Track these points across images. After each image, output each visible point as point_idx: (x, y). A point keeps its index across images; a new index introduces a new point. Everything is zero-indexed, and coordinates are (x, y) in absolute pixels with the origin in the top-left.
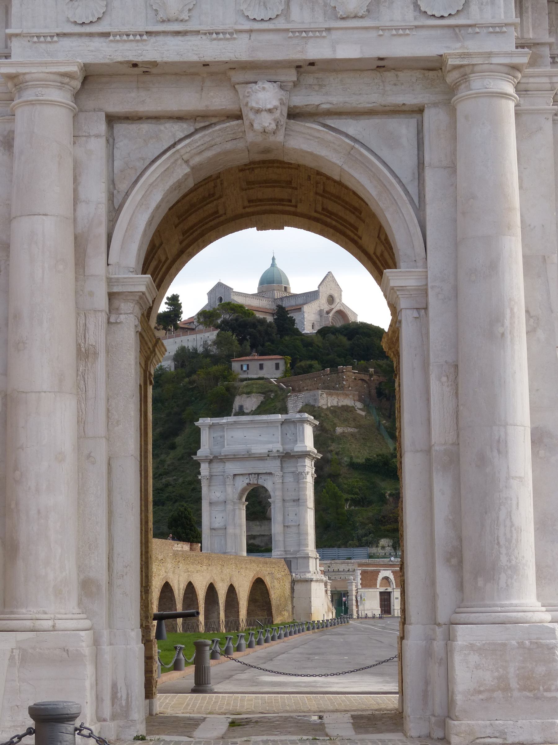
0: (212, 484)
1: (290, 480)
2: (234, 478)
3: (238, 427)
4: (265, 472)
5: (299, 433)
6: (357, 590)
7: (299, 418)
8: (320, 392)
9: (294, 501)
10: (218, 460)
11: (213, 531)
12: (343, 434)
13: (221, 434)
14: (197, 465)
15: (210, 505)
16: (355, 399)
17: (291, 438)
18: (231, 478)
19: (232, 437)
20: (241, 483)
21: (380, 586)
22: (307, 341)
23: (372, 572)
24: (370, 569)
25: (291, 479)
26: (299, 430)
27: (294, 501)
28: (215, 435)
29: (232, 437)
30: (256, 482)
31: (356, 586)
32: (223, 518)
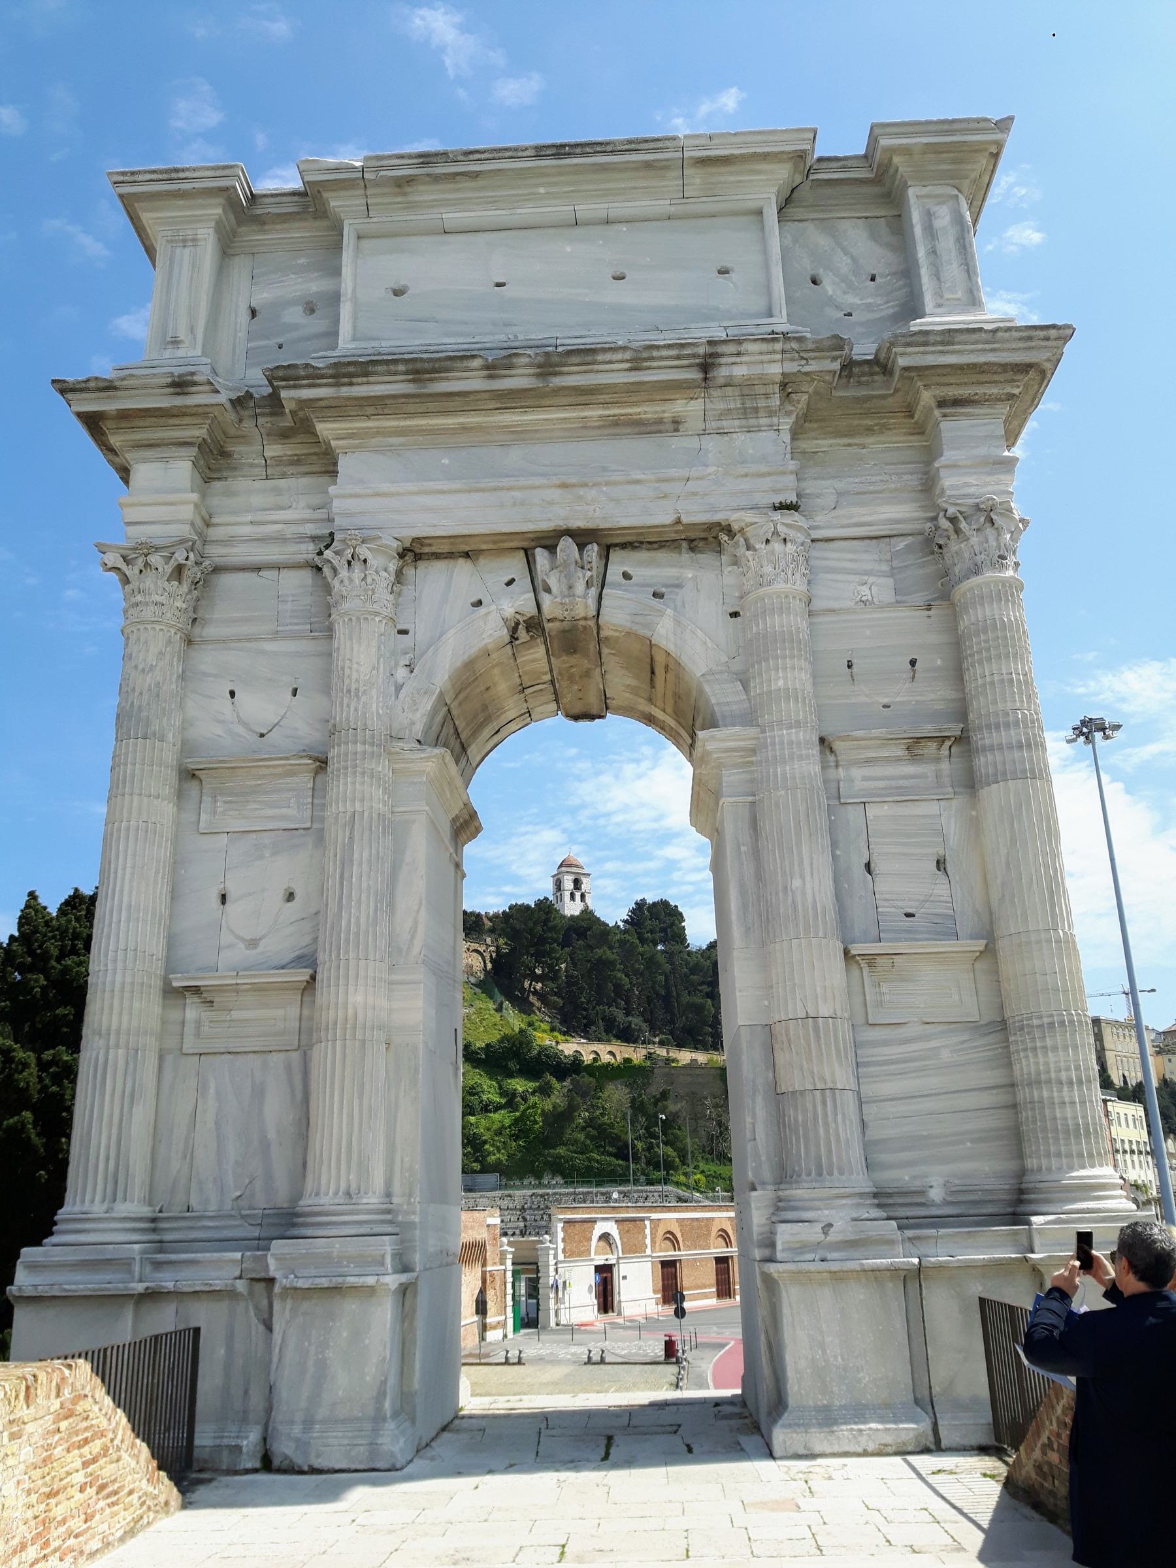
0: (210, 631)
3: (452, 217)
4: (668, 519)
5: (934, 252)
6: (556, 1264)
10: (274, 450)
11: (193, 1011)
13: (316, 285)
15: (180, 795)
17: (852, 299)
18: (383, 565)
19: (398, 293)
21: (596, 1254)
25: (881, 589)
26: (931, 232)
28: (262, 297)
29: (398, 293)
31: (555, 1256)
32: (290, 897)
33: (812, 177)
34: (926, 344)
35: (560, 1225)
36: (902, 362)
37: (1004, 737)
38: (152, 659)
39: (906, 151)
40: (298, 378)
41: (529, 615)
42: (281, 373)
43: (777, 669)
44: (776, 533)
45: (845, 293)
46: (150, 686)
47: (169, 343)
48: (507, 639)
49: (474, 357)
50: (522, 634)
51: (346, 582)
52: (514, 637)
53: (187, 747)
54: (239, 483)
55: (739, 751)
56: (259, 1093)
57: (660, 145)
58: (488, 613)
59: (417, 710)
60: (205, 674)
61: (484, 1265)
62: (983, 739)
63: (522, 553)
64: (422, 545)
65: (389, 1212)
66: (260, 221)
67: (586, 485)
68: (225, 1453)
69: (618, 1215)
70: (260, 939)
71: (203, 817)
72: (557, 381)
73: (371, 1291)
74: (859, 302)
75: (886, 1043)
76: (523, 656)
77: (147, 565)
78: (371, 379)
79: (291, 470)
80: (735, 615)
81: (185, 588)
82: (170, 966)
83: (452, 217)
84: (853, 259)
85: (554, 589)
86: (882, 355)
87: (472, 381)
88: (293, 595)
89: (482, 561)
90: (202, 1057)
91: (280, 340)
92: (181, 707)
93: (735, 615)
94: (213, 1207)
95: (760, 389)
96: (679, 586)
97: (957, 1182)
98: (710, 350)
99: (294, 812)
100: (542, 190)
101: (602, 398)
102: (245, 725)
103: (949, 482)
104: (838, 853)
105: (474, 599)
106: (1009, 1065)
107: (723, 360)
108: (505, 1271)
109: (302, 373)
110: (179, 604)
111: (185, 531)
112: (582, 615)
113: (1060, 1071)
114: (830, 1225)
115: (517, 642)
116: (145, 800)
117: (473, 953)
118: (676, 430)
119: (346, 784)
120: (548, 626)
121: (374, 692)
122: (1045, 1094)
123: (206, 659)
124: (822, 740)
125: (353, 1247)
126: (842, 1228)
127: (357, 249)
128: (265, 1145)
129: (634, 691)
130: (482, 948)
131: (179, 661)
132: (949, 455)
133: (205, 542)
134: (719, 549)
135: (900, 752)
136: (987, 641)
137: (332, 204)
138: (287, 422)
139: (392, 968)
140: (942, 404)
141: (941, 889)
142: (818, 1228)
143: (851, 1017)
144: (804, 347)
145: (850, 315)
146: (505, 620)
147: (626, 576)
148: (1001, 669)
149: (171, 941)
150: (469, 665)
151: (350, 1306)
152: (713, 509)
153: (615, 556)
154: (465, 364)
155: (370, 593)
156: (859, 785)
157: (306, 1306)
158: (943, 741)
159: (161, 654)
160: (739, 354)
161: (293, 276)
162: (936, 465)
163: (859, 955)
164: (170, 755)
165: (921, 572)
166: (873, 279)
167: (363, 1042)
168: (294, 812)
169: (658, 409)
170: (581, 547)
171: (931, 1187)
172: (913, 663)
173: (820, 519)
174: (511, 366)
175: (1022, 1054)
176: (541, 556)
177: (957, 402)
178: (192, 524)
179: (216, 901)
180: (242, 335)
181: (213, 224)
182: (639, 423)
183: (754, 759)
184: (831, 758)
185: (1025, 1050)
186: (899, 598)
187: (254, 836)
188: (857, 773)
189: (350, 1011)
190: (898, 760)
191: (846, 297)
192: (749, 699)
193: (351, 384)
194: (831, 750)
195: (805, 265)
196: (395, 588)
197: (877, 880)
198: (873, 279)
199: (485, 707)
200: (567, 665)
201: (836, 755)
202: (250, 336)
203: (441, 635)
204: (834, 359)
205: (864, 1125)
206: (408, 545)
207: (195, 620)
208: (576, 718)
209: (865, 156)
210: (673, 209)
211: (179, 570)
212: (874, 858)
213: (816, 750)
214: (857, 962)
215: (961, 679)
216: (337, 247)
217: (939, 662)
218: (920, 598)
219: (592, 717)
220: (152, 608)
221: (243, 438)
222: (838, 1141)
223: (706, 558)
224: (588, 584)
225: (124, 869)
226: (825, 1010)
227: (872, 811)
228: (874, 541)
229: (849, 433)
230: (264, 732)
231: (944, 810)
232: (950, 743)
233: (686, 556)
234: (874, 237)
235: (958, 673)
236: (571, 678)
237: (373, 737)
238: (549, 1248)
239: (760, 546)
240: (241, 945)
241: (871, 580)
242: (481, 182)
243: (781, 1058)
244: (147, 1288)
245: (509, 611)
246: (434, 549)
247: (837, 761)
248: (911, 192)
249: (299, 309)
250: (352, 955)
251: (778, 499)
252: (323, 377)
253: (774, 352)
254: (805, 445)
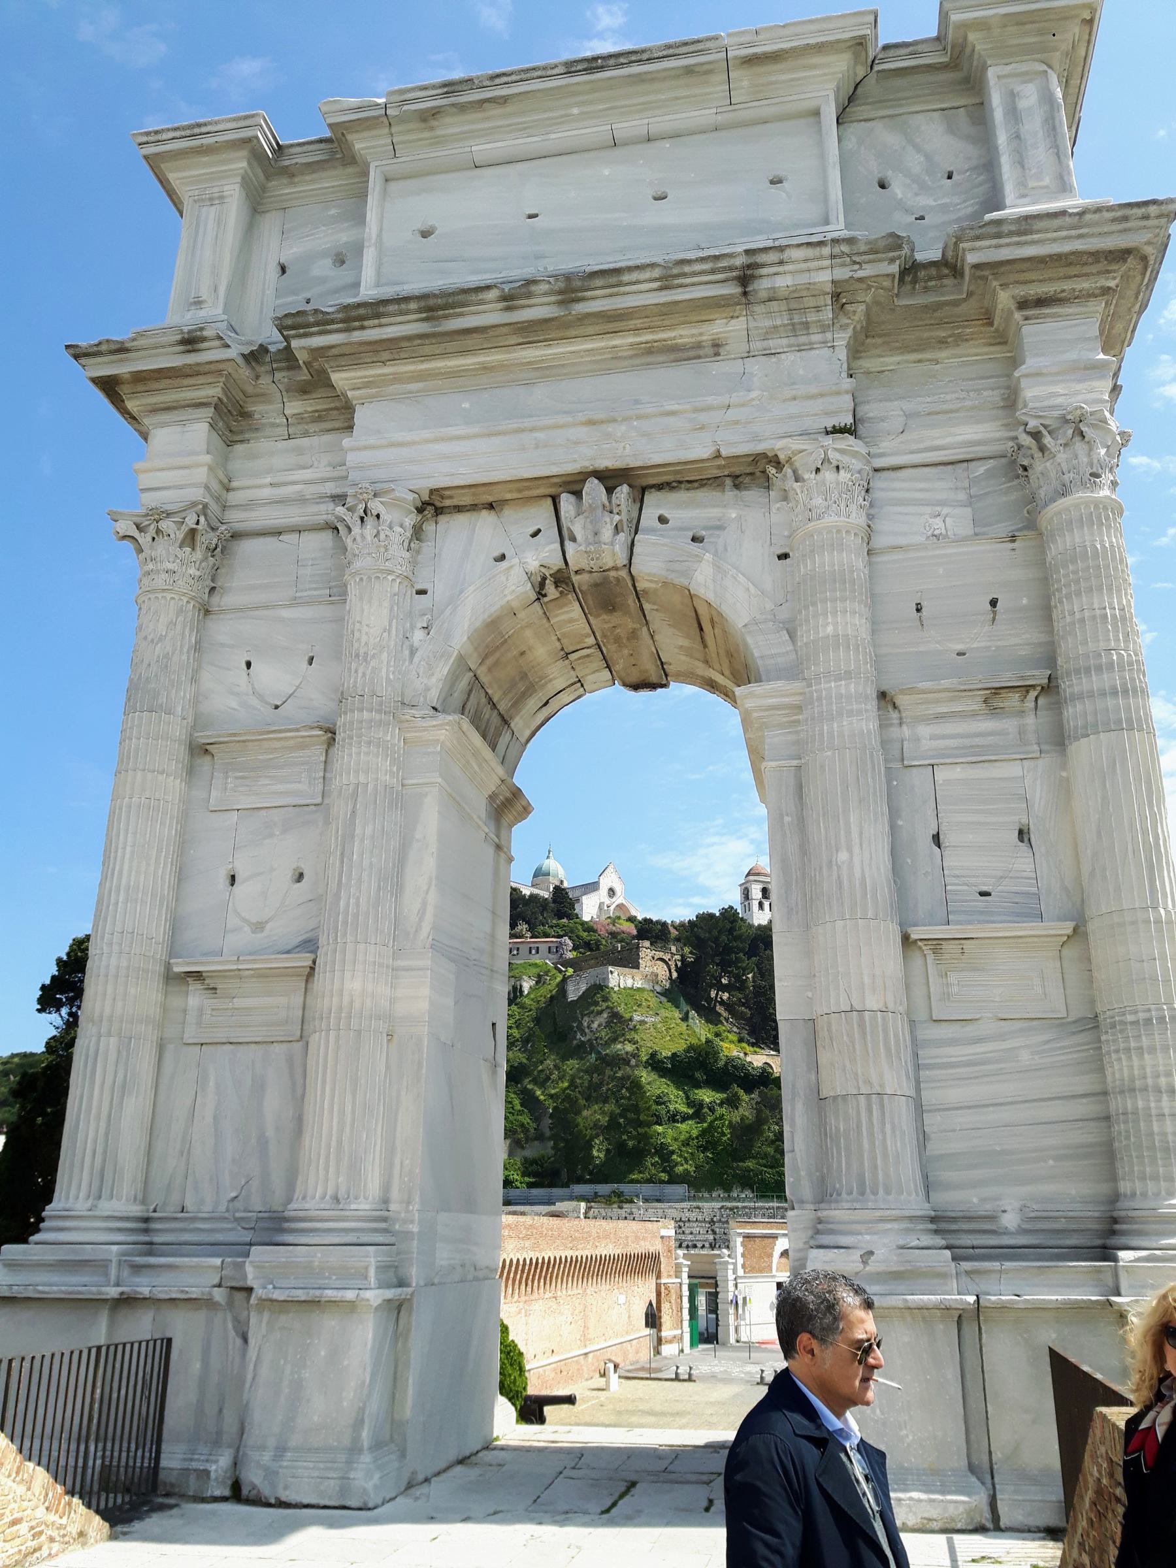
1: (938, 525)
2: (418, 532)
3: (482, 149)
6: (735, 1279)
8: (610, 968)
10: (294, 407)
11: (195, 998)
12: (642, 1022)
13: (344, 236)
15: (191, 772)
17: (925, 201)
19: (425, 234)
22: (589, 928)
25: (957, 521)
26: (1013, 114)
29: (425, 234)
33: (876, 68)
34: (999, 236)
35: (739, 1240)
36: (971, 258)
37: (1096, 682)
38: (161, 629)
39: (982, 25)
40: (308, 326)
41: (555, 568)
42: (289, 322)
43: (825, 614)
44: (826, 460)
45: (916, 195)
46: (159, 657)
47: (191, 304)
48: (533, 596)
49: (488, 288)
50: (551, 591)
51: (359, 539)
52: (541, 594)
53: (199, 722)
54: (261, 445)
55: (783, 709)
56: (259, 1087)
57: (700, 46)
58: (511, 567)
59: (433, 674)
60: (222, 645)
61: (659, 1277)
62: (1071, 686)
63: (549, 501)
64: (443, 498)
65: (385, 1219)
66: (289, 173)
67: (614, 420)
68: (192, 1478)
70: (267, 922)
71: (214, 794)
72: (581, 308)
73: (351, 1307)
74: (934, 203)
75: (954, 1042)
76: (557, 616)
77: (158, 531)
78: (383, 321)
79: (313, 428)
80: (784, 556)
81: (199, 555)
82: (173, 951)
83: (482, 149)
84: (928, 157)
85: (579, 537)
86: (950, 254)
87: (489, 315)
88: (312, 559)
89: (507, 512)
90: (204, 1046)
91: (308, 295)
92: (194, 680)
93: (784, 556)
94: (208, 1207)
95: (810, 302)
96: (721, 528)
97: (1035, 1207)
98: (750, 260)
99: (305, 788)
100: (575, 111)
101: (632, 323)
102: (261, 698)
103: (1031, 392)
104: (900, 823)
105: (497, 554)
106: (1101, 1070)
107: (764, 271)
108: (681, 1284)
109: (311, 319)
110: (192, 571)
111: (198, 494)
112: (610, 564)
113: (1158, 1076)
114: (871, 1253)
115: (546, 599)
116: (149, 775)
117: (658, 962)
118: (717, 354)
119: (350, 755)
120: (576, 579)
121: (385, 656)
122: (1140, 1104)
123: (221, 630)
124: (883, 695)
125: (336, 1256)
126: (885, 1255)
127: (385, 192)
128: (263, 1143)
129: (689, 652)
130: (667, 957)
131: (191, 630)
132: (1031, 363)
133: (224, 508)
134: (767, 483)
135: (975, 704)
136: (1076, 572)
137: (357, 146)
138: (304, 375)
139: (395, 956)
140: (1023, 305)
141: (1022, 861)
142: (856, 1255)
143: (908, 1013)
144: (855, 249)
145: (922, 218)
146: (529, 576)
147: (663, 520)
148: (1093, 603)
149: (176, 925)
150: (493, 625)
151: (329, 1323)
152: (757, 439)
153: (650, 498)
154: (481, 296)
155: (382, 550)
156: (926, 745)
157: (284, 1320)
158: (1028, 692)
159: (172, 624)
160: (781, 263)
161: (323, 228)
162: (1016, 374)
163: (921, 940)
164: (177, 729)
165: (1004, 499)
166: (950, 177)
167: (359, 1032)
168: (305, 788)
169: (694, 331)
170: (610, 491)
171: (1004, 1211)
172: (994, 603)
173: (885, 445)
174: (529, 295)
175: (1114, 1056)
176: (567, 503)
177: (1041, 302)
178: (207, 487)
179: (223, 881)
180: (270, 292)
181: (239, 179)
182: (675, 349)
183: (801, 717)
184: (894, 715)
185: (1117, 1051)
186: (977, 530)
187: (263, 812)
188: (924, 731)
189: (346, 1000)
190: (974, 715)
191: (918, 198)
192: (795, 650)
193: (363, 328)
194: (895, 707)
195: (871, 168)
196: (412, 545)
197: (946, 853)
198: (950, 177)
199: (524, 676)
200: (610, 625)
201: (900, 711)
202: (279, 293)
203: (461, 592)
204: (892, 260)
205: (923, 1138)
206: (426, 498)
207: (213, 589)
208: (636, 687)
209: (938, 39)
210: (719, 117)
211: (192, 536)
212: (942, 828)
213: (872, 704)
214: (920, 948)
215: (1049, 618)
216: (363, 195)
217: (1025, 601)
218: (1003, 529)
219: (653, 686)
220: (164, 576)
221: (263, 397)
222: (885, 1155)
223: (753, 495)
224: (617, 529)
225: (124, 848)
226: (872, 1003)
227: (941, 775)
228: (950, 467)
229: (921, 346)
230: (279, 703)
231: (1028, 772)
232: (1036, 693)
233: (730, 494)
234: (951, 130)
235: (1046, 612)
236: (617, 640)
237: (381, 704)
238: (727, 1263)
239: (809, 476)
240: (247, 929)
241: (946, 510)
242: (509, 108)
243: (824, 1057)
244: (122, 1293)
245: (533, 564)
246: (455, 502)
247: (901, 718)
248: (991, 73)
249: (328, 262)
250: (349, 938)
251: (830, 423)
252: (332, 322)
253: (821, 258)
254: (869, 364)
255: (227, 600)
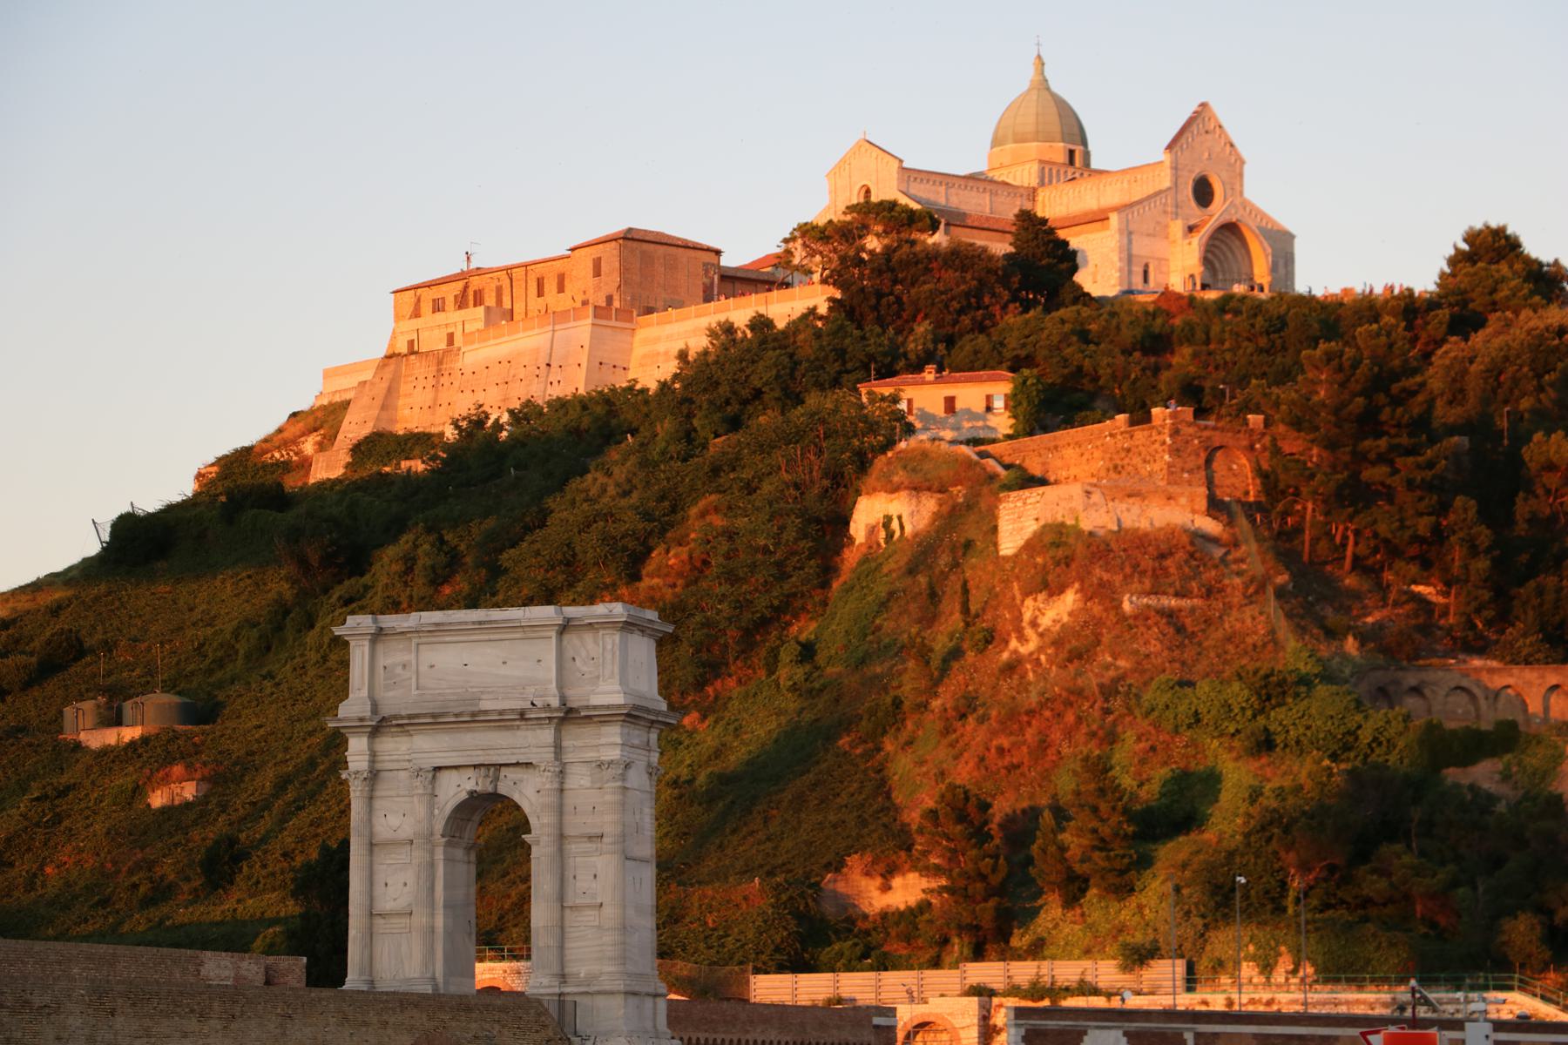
1: (582, 782)
2: (434, 777)
3: (448, 639)
7: (606, 616)
9: (590, 838)
14: (337, 742)
16: (1196, 507)
17: (585, 669)
19: (432, 666)
20: (455, 789)
23: (1061, 1032)
24: (1051, 1024)
25: (586, 782)
27: (590, 838)
30: (490, 789)
32: (405, 884)
69: (1126, 1024)
83: (448, 639)
255: (378, 793)
